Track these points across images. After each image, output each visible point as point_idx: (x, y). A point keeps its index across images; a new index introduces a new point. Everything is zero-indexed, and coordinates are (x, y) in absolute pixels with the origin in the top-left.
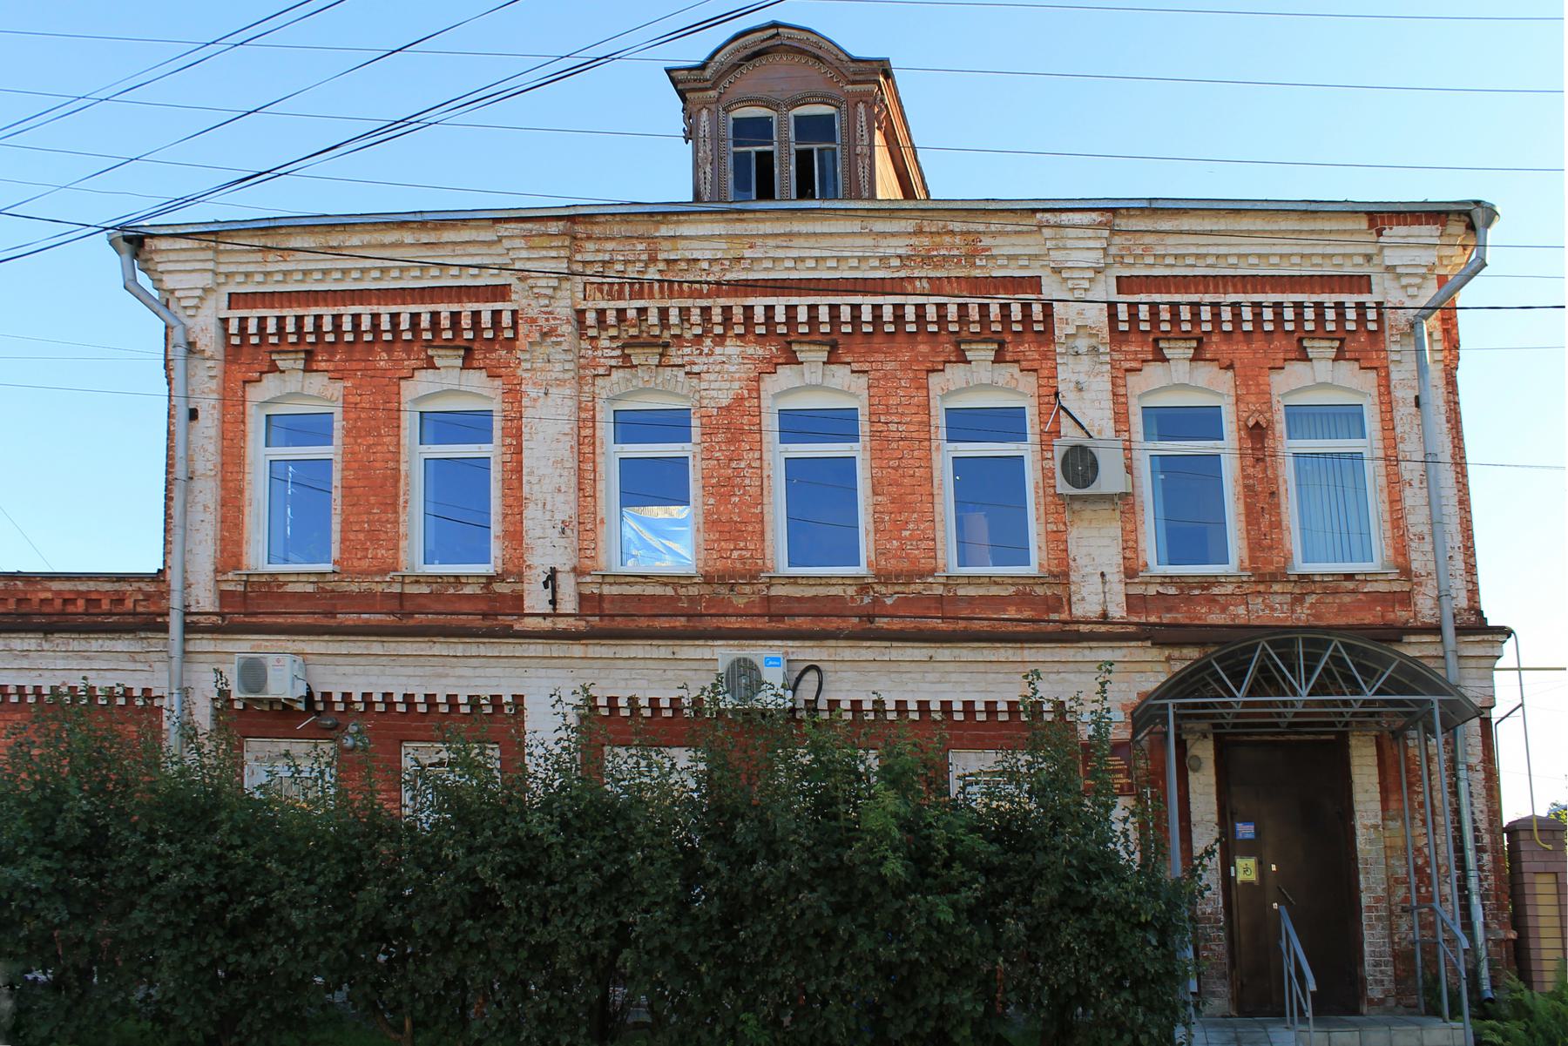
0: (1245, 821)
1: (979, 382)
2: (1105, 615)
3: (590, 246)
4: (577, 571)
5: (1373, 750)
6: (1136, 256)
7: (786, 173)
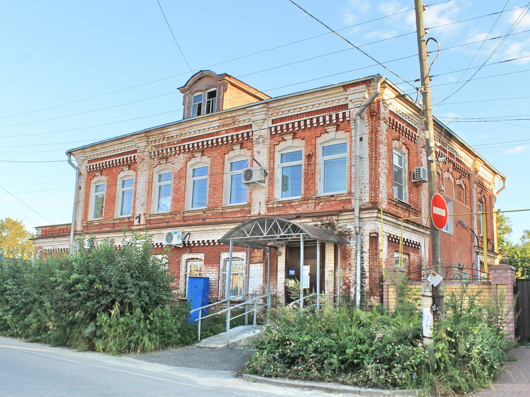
0: (292, 270)
1: (238, 154)
2: (259, 214)
3: (151, 137)
4: (145, 214)
5: (333, 248)
6: (277, 113)
7: (204, 108)
